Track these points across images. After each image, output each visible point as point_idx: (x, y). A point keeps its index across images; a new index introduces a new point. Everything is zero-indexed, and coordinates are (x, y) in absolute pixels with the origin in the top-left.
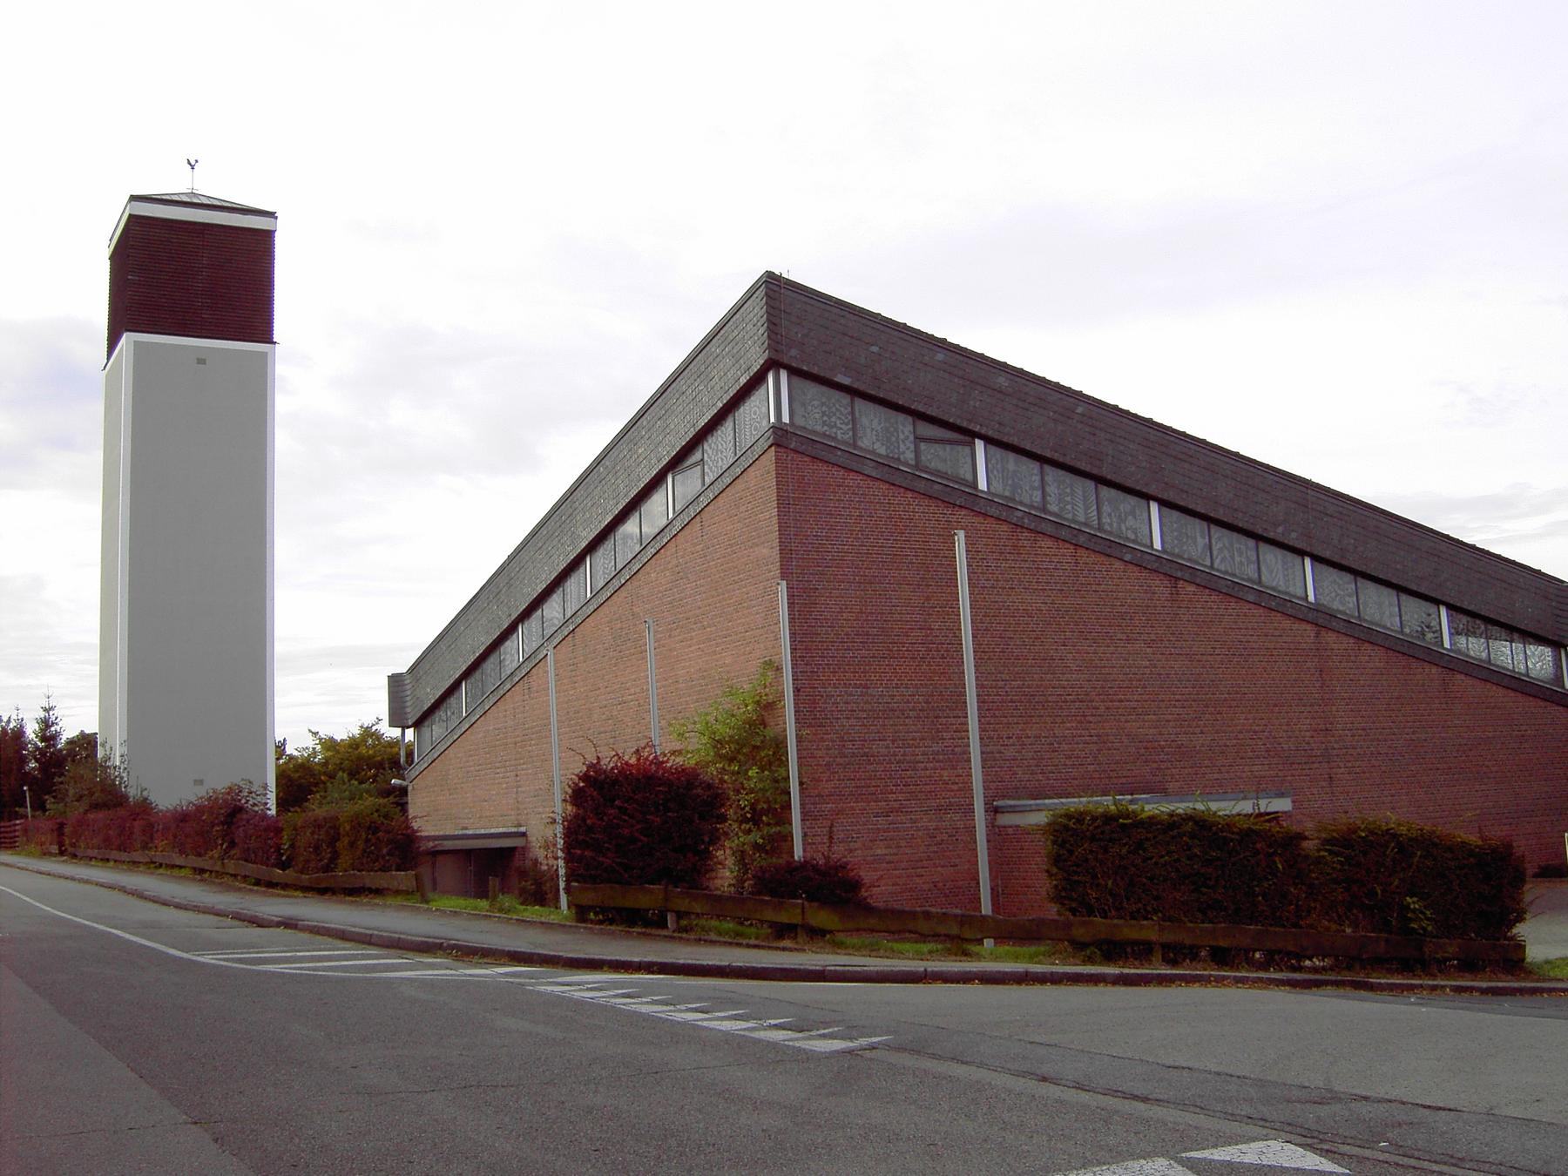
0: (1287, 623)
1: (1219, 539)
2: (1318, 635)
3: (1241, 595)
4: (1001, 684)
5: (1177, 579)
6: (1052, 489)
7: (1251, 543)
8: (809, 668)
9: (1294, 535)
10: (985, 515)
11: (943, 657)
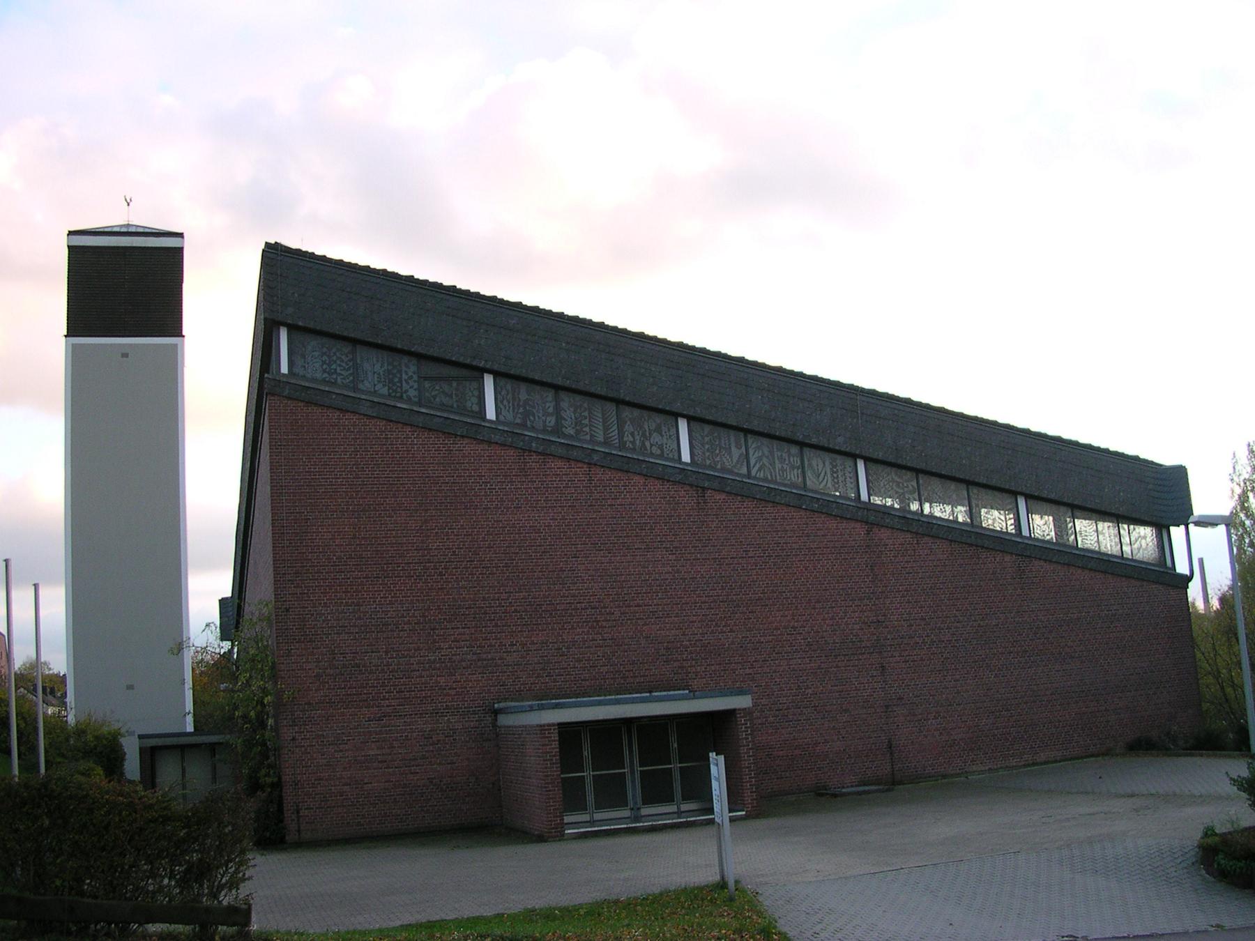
0: (832, 524)
1: (758, 448)
2: (868, 532)
3: (778, 499)
4: (504, 596)
5: (704, 489)
6: (569, 414)
7: (795, 450)
8: (299, 590)
9: (840, 440)
10: (490, 443)
11: (441, 574)
